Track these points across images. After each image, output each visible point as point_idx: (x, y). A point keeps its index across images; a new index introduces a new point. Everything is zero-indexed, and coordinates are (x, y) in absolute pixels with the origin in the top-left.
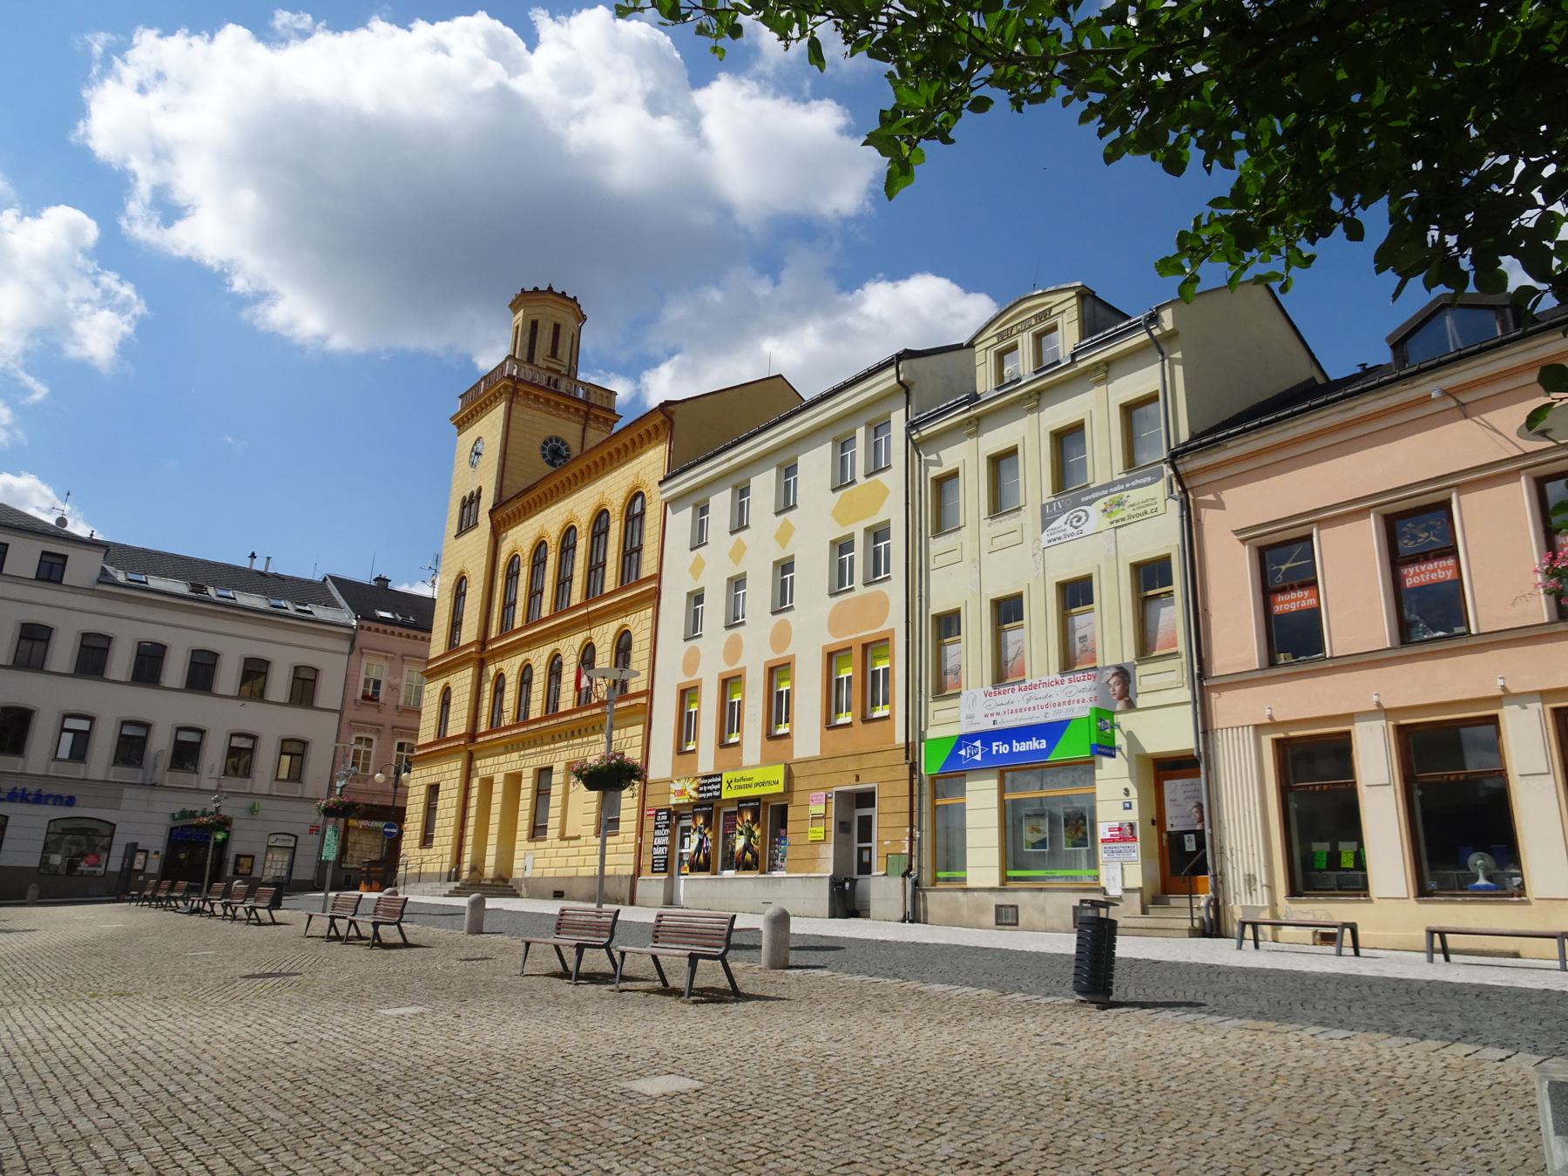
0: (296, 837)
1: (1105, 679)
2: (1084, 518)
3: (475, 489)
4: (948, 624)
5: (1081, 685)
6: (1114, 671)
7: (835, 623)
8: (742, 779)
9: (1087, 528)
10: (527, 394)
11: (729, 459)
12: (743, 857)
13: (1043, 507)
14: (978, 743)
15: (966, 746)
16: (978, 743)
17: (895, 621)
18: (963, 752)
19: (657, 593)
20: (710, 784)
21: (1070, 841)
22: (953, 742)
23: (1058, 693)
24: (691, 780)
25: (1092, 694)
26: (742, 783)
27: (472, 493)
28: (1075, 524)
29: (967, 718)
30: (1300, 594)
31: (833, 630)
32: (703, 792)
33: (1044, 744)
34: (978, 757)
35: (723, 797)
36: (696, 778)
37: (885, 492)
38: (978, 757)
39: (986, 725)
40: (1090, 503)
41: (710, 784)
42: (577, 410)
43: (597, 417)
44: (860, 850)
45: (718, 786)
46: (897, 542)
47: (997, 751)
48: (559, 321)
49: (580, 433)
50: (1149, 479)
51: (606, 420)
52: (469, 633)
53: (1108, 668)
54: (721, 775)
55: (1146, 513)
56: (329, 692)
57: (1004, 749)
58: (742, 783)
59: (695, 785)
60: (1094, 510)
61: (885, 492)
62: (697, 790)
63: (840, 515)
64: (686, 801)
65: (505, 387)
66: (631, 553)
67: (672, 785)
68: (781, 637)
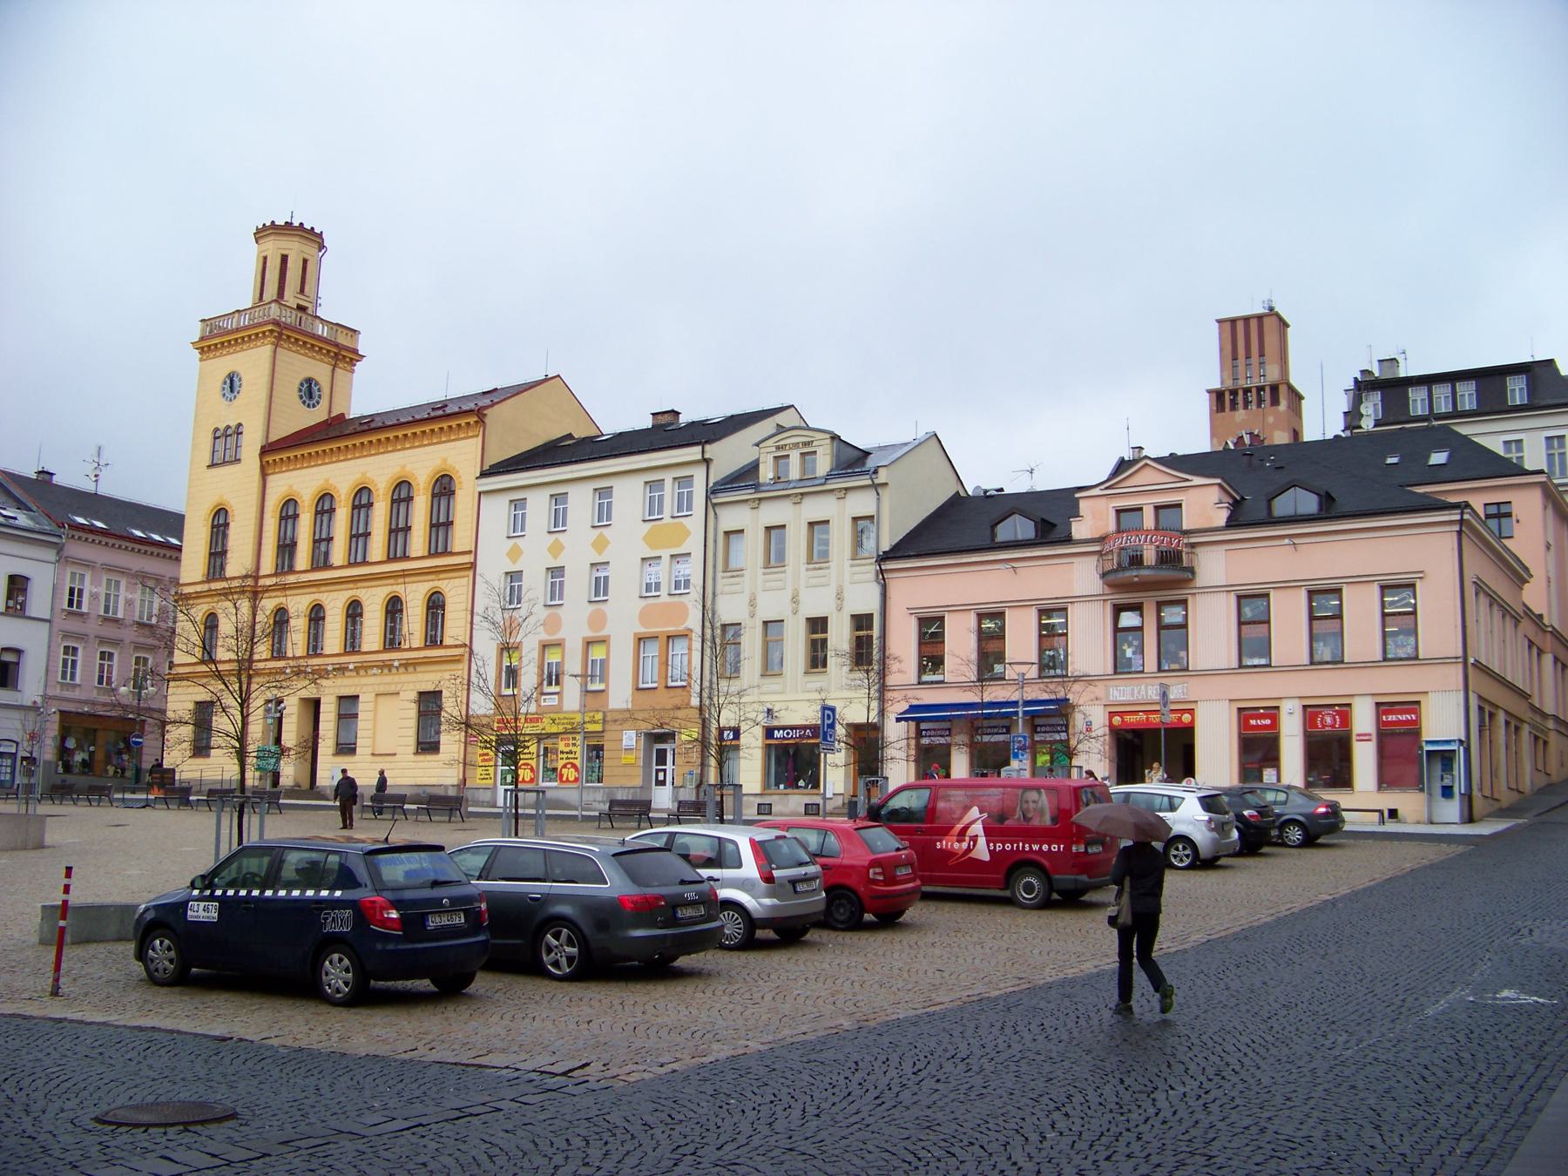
0: (17, 743)
3: (233, 424)
7: (644, 616)
10: (289, 337)
19: (473, 566)
27: (228, 427)
31: (643, 624)
37: (688, 533)
42: (328, 351)
43: (344, 357)
44: (657, 771)
48: (307, 257)
49: (330, 374)
51: (351, 359)
52: (238, 563)
56: (39, 600)
61: (688, 533)
63: (649, 540)
65: (271, 331)
66: (441, 526)
68: (598, 620)
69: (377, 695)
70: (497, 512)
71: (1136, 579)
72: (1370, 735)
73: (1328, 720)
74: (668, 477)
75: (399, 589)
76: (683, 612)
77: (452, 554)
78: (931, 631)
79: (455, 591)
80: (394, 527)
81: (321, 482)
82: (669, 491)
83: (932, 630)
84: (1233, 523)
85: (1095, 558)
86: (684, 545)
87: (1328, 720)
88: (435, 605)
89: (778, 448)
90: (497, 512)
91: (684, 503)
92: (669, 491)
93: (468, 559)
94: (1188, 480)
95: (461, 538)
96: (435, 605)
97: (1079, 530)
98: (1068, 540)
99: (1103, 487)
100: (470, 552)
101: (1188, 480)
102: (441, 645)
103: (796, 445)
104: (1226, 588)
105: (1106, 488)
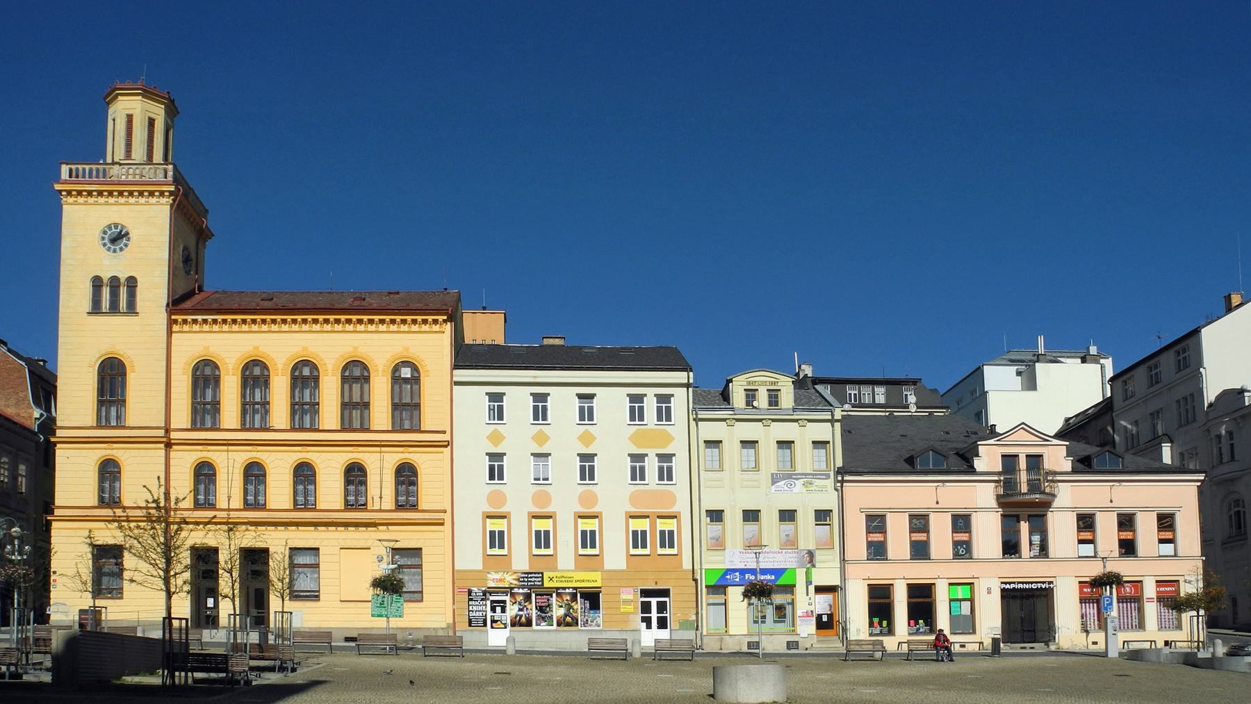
1: (802, 555)
2: (793, 485)
4: (716, 516)
5: (791, 555)
6: (806, 552)
7: (633, 499)
8: (563, 577)
9: (796, 490)
11: (535, 377)
12: (564, 620)
13: (772, 474)
14: (737, 574)
15: (730, 574)
16: (737, 574)
17: (682, 506)
18: (728, 577)
20: (531, 577)
21: (777, 617)
22: (723, 571)
23: (780, 557)
24: (510, 573)
25: (796, 559)
26: (563, 579)
28: (789, 485)
29: (730, 562)
30: (878, 535)
32: (522, 581)
33: (773, 577)
34: (738, 580)
35: (545, 586)
36: (515, 573)
38: (738, 580)
39: (742, 566)
40: (797, 479)
41: (531, 577)
45: (540, 579)
46: (679, 466)
47: (748, 578)
50: (824, 477)
53: (804, 550)
54: (542, 573)
55: (822, 489)
57: (752, 577)
58: (563, 579)
59: (515, 576)
60: (799, 483)
62: (518, 580)
63: (634, 439)
64: (507, 586)
65: (171, 193)
67: (488, 575)
69: (341, 548)
70: (473, 401)
71: (1037, 500)
72: (1153, 598)
73: (1128, 590)
74: (651, 392)
75: (312, 456)
76: (672, 499)
77: (368, 430)
78: (876, 522)
79: (428, 464)
80: (347, 400)
81: (251, 349)
82: (650, 405)
83: (875, 524)
84: (1075, 471)
85: (993, 485)
86: (669, 447)
87: (1128, 590)
88: (406, 476)
89: (749, 383)
90: (473, 401)
91: (664, 414)
92: (650, 405)
93: (446, 437)
94: (1048, 441)
95: (432, 416)
96: (406, 476)
97: (979, 464)
98: (971, 470)
99: (996, 439)
100: (444, 432)
101: (1048, 441)
102: (363, 507)
103: (764, 383)
104: (1072, 509)
105: (998, 440)
